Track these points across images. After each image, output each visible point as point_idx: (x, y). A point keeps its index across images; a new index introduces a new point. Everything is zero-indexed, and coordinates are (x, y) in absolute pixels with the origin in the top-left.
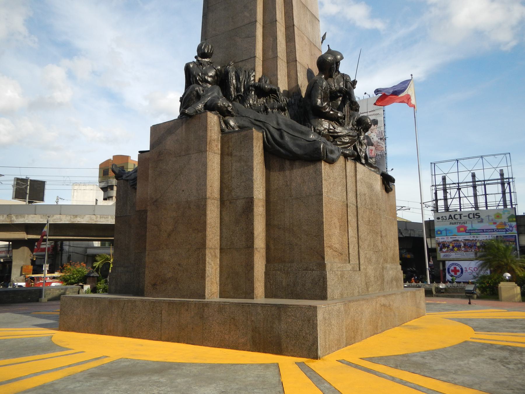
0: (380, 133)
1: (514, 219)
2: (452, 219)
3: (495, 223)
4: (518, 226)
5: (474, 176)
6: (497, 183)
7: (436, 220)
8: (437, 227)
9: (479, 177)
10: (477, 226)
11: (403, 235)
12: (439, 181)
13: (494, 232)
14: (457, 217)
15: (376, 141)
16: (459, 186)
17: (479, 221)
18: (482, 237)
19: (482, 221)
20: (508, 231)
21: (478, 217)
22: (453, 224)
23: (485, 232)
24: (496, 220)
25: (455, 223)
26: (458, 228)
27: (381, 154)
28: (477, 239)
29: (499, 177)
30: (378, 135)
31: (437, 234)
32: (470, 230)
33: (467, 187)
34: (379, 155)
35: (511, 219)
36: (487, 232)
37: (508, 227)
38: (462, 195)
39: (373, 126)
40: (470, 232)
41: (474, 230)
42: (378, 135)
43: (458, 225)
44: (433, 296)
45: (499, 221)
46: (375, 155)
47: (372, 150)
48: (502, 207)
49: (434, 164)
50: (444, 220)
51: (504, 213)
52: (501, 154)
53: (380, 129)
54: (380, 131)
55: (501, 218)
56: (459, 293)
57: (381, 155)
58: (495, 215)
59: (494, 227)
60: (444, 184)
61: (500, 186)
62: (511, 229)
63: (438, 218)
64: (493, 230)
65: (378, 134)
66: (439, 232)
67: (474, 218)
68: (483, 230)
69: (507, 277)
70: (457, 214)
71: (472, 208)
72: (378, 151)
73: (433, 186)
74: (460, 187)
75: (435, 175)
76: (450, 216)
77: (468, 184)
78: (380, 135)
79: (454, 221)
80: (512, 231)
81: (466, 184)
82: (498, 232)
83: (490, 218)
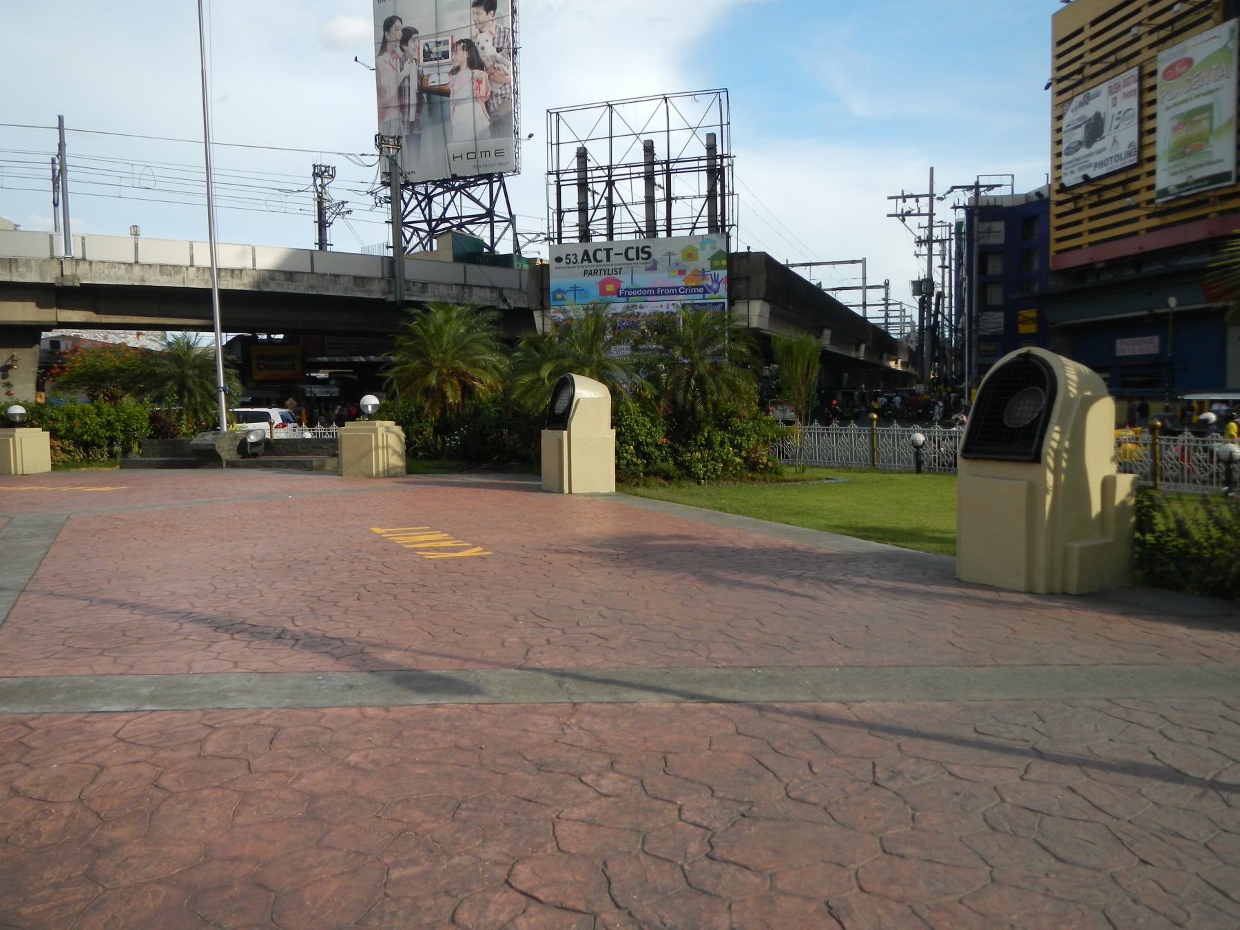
0: (502, 34)
1: (724, 262)
2: (590, 261)
3: (682, 272)
4: (731, 280)
5: (649, 148)
6: (698, 169)
7: (554, 265)
8: (555, 282)
9: (660, 154)
10: (645, 279)
11: (509, 305)
12: (569, 160)
13: (678, 294)
14: (601, 255)
15: (492, 56)
16: (610, 176)
17: (649, 266)
18: (651, 307)
19: (654, 268)
20: (708, 293)
21: (646, 256)
22: (590, 274)
23: (660, 294)
24: (685, 263)
25: (596, 272)
26: (602, 285)
27: (504, 92)
28: (642, 311)
29: (703, 152)
30: (496, 41)
31: (555, 299)
32: (627, 289)
33: (631, 176)
34: (497, 95)
35: (716, 263)
36: (664, 294)
37: (710, 283)
38: (616, 200)
39: (485, 13)
40: (627, 296)
41: (637, 289)
42: (496, 41)
43: (602, 277)
44: (221, 466)
45: (691, 266)
46: (489, 94)
47: (480, 82)
48: (706, 232)
49: (557, 113)
50: (572, 264)
51: (703, 247)
52: (707, 92)
53: (503, 24)
54: (502, 30)
55: (697, 259)
56: (300, 454)
57: (502, 95)
58: (683, 251)
59: (679, 282)
60: (582, 168)
61: (704, 175)
62: (715, 286)
63: (559, 260)
64: (677, 291)
65: (497, 36)
66: (559, 296)
67: (638, 258)
68: (656, 289)
69: (370, 408)
70: (600, 250)
71: (635, 232)
72: (495, 85)
73: (550, 173)
74: (613, 178)
75: (558, 144)
76: (586, 253)
77: (634, 170)
78: (501, 40)
79: (593, 266)
80: (716, 291)
81: (627, 171)
82: (688, 293)
83: (673, 259)
